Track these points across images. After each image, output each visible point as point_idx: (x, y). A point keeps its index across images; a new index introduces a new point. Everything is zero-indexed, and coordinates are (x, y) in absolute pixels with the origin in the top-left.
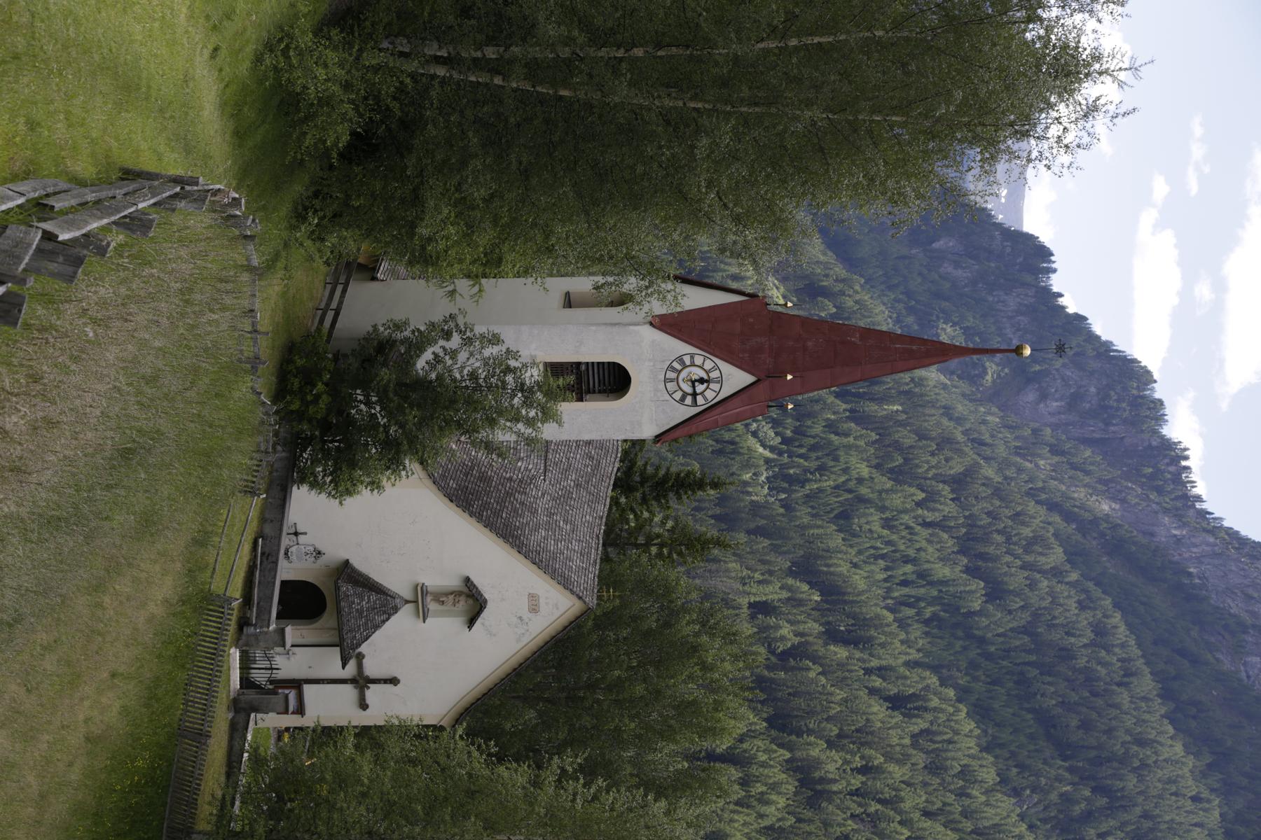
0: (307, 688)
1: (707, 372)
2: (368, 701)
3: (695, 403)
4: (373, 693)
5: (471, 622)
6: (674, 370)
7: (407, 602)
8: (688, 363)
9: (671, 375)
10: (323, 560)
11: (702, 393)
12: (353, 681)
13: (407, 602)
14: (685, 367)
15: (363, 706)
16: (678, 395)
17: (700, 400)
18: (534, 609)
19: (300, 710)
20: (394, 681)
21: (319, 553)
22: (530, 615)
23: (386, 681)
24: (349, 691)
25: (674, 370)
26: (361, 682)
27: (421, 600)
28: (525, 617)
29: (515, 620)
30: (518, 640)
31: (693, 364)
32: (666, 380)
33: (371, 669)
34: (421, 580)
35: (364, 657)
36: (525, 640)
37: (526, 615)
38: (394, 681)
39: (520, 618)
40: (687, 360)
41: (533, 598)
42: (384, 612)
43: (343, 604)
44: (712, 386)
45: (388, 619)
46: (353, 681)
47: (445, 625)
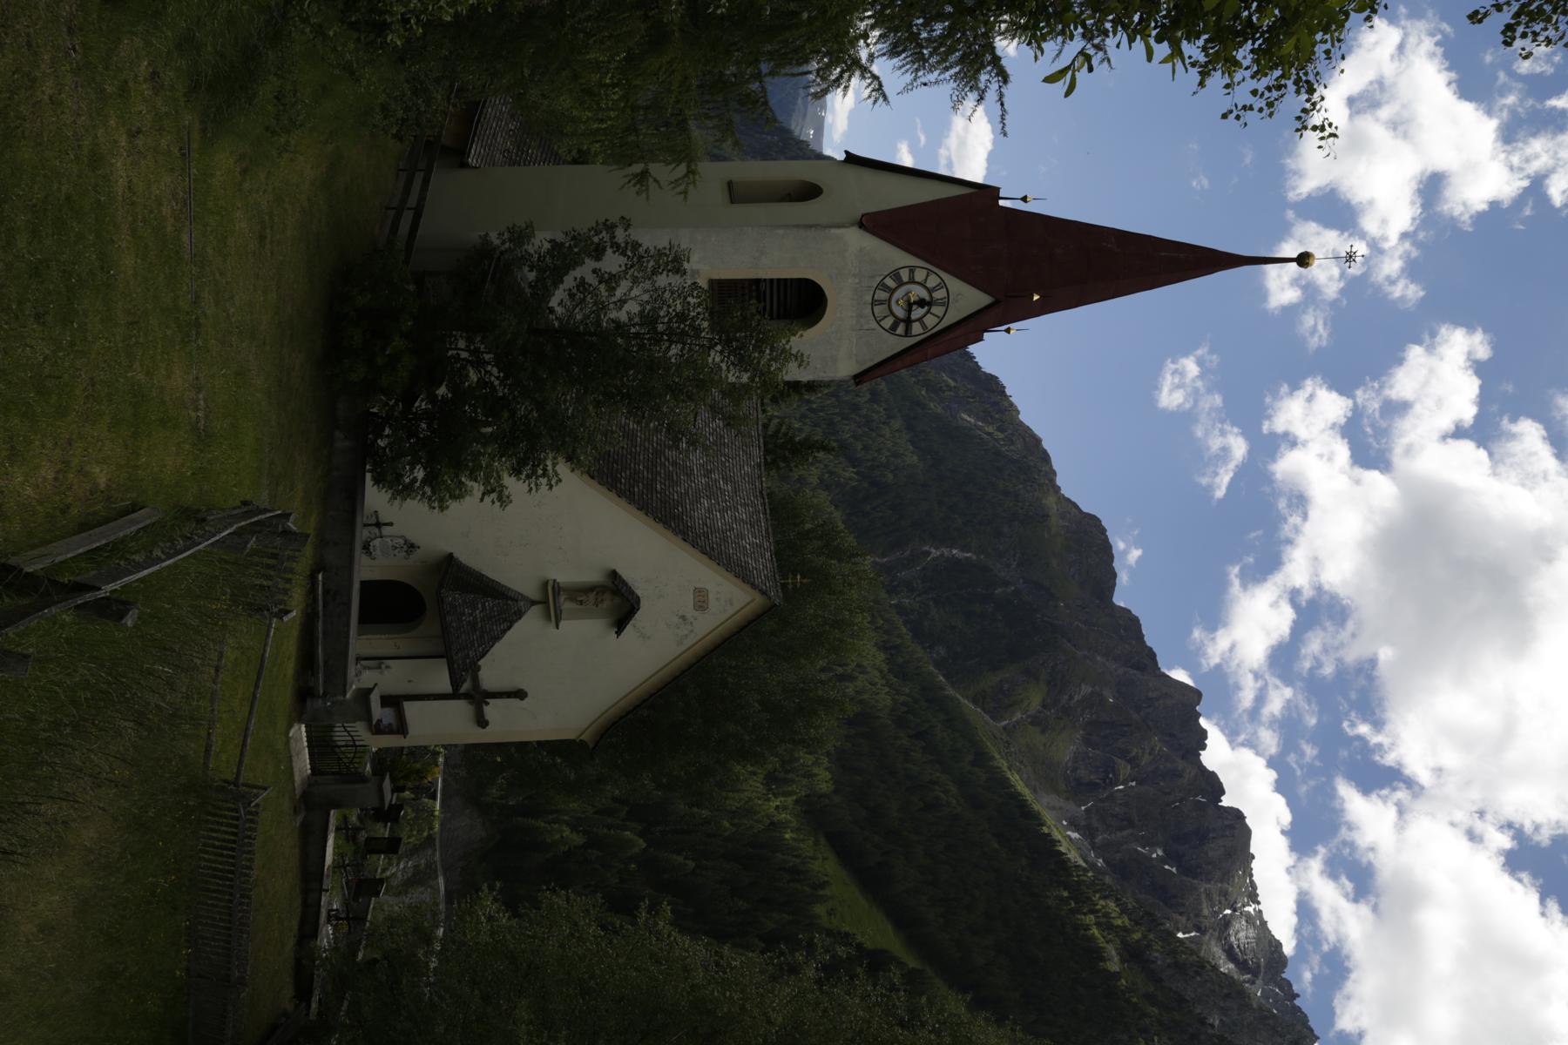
0: (410, 708)
1: (930, 291)
2: (488, 717)
3: (907, 333)
4: (493, 709)
6: (885, 288)
7: (533, 603)
8: (905, 279)
9: (882, 295)
10: (416, 555)
11: (920, 320)
13: (533, 603)
14: (901, 284)
15: (482, 722)
16: (888, 323)
17: (916, 328)
20: (520, 694)
22: (696, 614)
24: (461, 708)
25: (882, 286)
26: (479, 698)
27: (554, 600)
31: (912, 281)
32: (874, 303)
36: (688, 642)
37: (690, 613)
38: (520, 694)
39: (683, 617)
40: (905, 275)
43: (449, 618)
44: (935, 310)
46: (466, 696)
47: (584, 629)
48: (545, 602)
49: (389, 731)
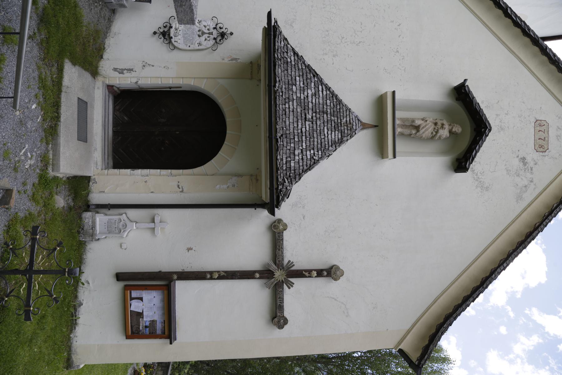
0: (183, 290)
4: (296, 296)
5: (461, 164)
12: (265, 274)
13: (365, 126)
18: (541, 146)
19: (168, 332)
20: (330, 272)
21: (223, 35)
22: (536, 155)
23: (320, 273)
24: (255, 293)
26: (277, 274)
28: (529, 159)
29: (516, 163)
30: (519, 198)
33: (295, 252)
34: (387, 89)
35: (285, 227)
36: (529, 197)
37: (532, 155)
38: (330, 272)
39: (523, 160)
41: (540, 126)
42: (337, 127)
43: (279, 71)
45: (341, 142)
46: (265, 274)
47: (419, 167)
48: (379, 126)
49: (151, 333)
